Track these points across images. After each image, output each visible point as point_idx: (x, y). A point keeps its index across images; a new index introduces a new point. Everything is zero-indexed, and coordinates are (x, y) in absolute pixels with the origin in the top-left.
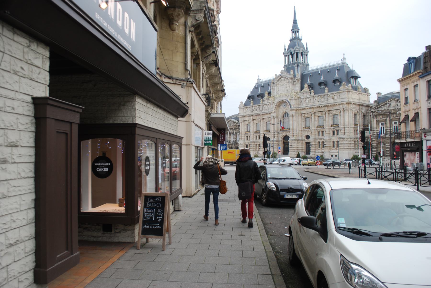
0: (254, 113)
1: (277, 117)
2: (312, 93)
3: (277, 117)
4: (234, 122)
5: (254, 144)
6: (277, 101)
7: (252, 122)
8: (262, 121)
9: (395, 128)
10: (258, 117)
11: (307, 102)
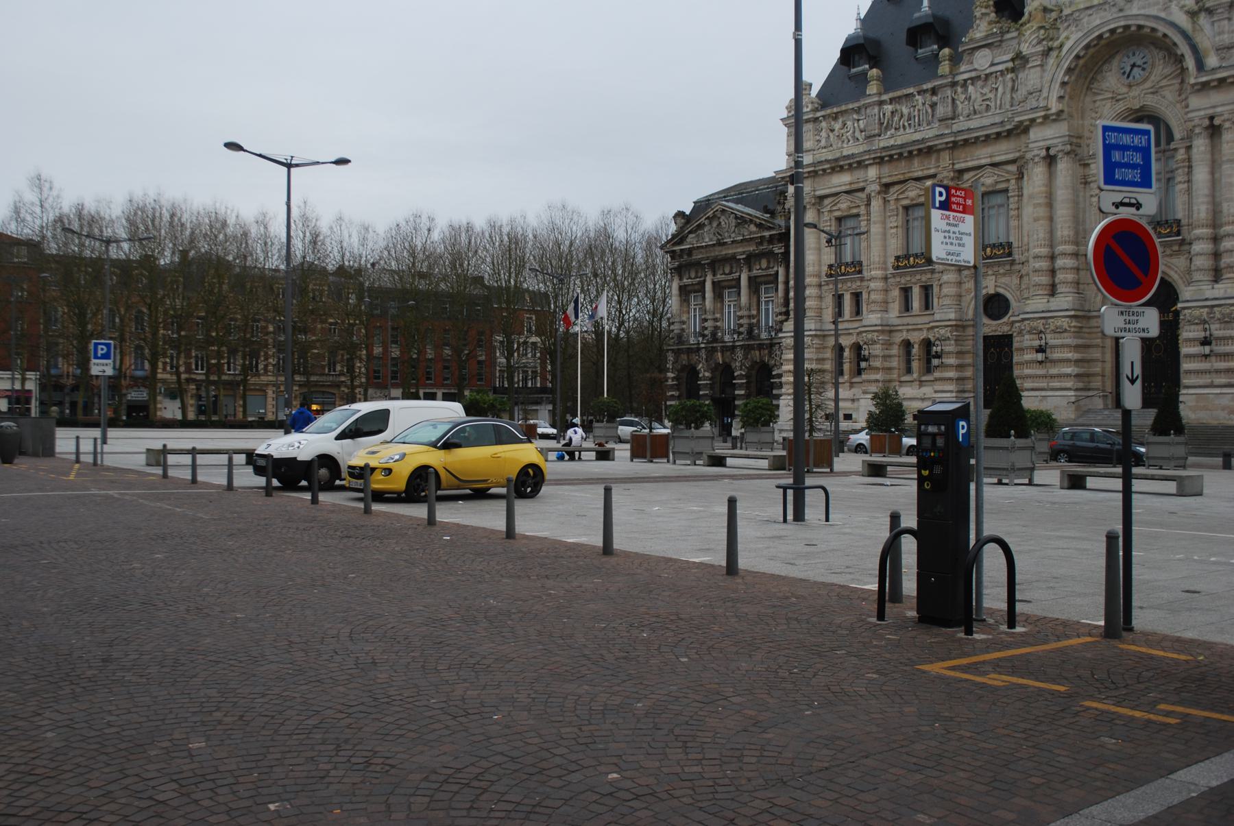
0: (884, 142)
1: (1075, 149)
3: (1075, 149)
4: (742, 221)
5: (888, 344)
6: (1073, 40)
7: (876, 204)
10: (917, 168)
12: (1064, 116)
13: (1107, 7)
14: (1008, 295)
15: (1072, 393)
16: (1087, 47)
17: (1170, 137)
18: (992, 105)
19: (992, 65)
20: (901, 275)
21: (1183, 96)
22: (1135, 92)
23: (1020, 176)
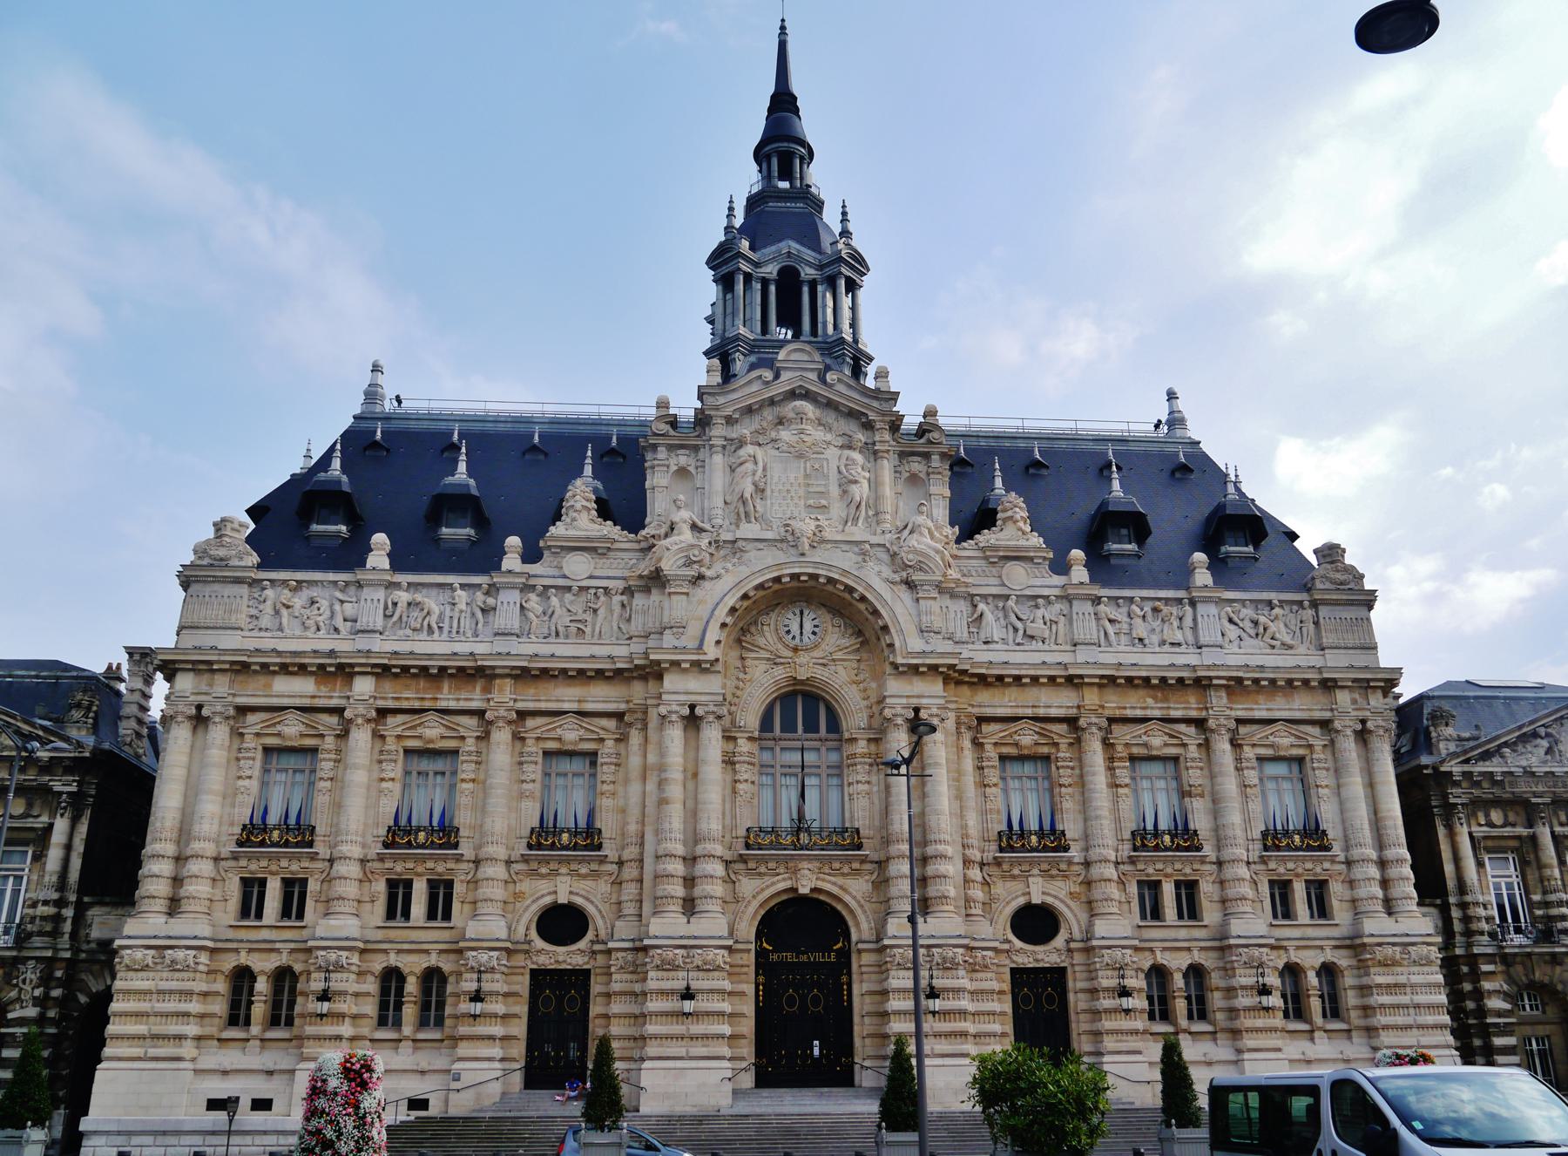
2: (1080, 574)
7: (361, 737)
8: (501, 736)
9: (1501, 908)
10: (448, 697)
11: (1038, 627)
12: (719, 667)
13: (784, 545)
14: (590, 909)
15: (726, 1064)
16: (760, 587)
17: (834, 725)
18: (588, 630)
19: (591, 577)
20: (395, 858)
21: (861, 677)
22: (803, 658)
23: (622, 739)
